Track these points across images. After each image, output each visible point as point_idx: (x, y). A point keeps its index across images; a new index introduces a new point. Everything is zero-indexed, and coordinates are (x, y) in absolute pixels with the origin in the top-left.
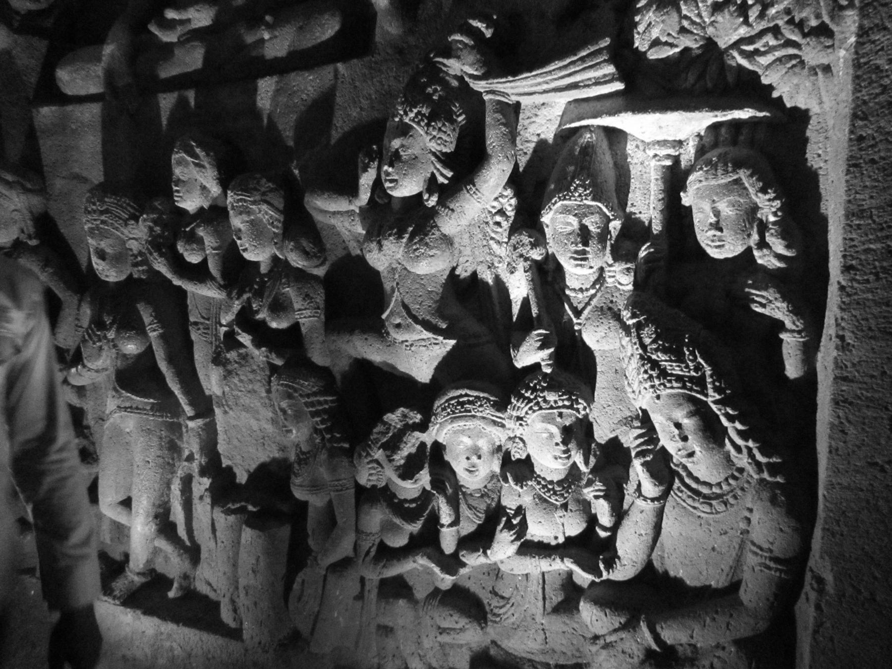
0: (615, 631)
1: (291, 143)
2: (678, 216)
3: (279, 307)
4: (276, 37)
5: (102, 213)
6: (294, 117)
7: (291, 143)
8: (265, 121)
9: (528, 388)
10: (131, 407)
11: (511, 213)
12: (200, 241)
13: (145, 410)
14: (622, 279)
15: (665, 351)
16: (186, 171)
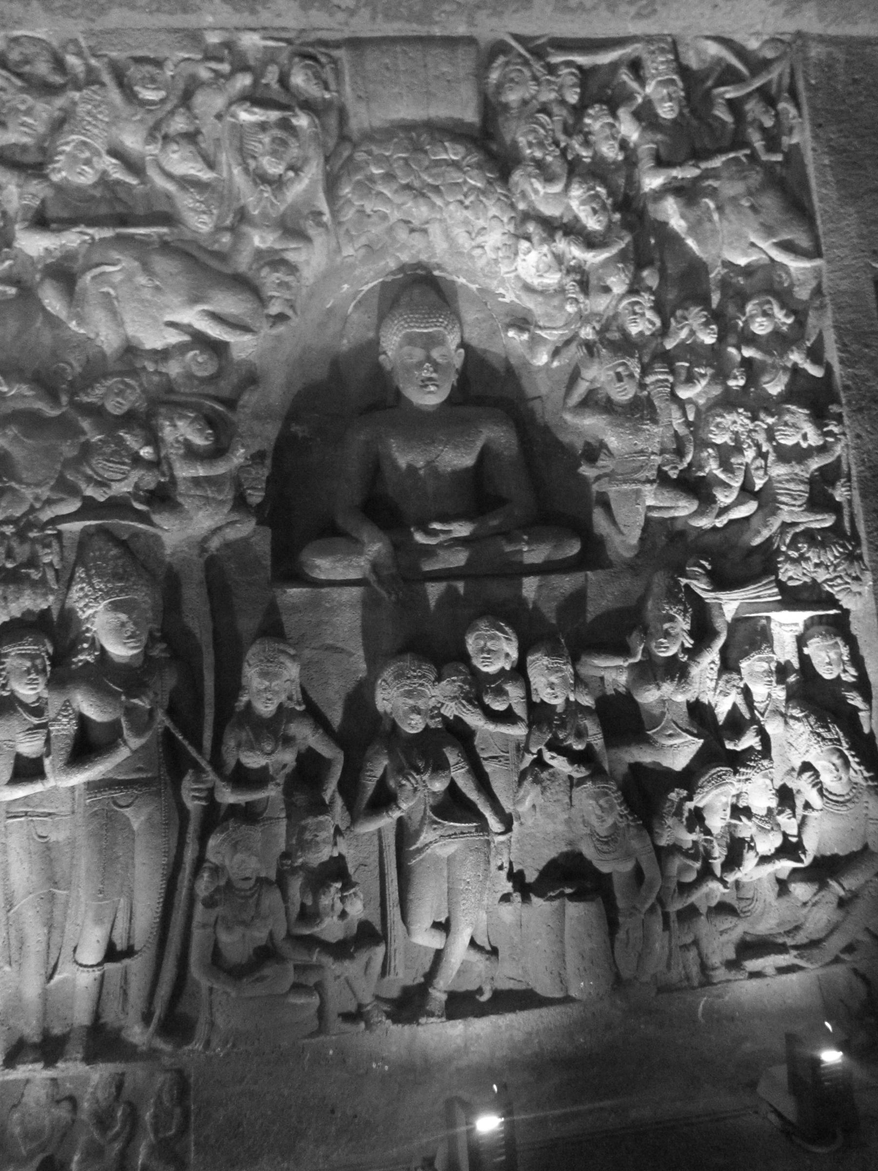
0: (815, 894)
1: (554, 621)
2: (805, 660)
3: (580, 734)
5: (420, 677)
6: (554, 604)
7: (554, 621)
8: (531, 606)
9: (751, 760)
11: (718, 662)
14: (780, 693)
15: (822, 727)
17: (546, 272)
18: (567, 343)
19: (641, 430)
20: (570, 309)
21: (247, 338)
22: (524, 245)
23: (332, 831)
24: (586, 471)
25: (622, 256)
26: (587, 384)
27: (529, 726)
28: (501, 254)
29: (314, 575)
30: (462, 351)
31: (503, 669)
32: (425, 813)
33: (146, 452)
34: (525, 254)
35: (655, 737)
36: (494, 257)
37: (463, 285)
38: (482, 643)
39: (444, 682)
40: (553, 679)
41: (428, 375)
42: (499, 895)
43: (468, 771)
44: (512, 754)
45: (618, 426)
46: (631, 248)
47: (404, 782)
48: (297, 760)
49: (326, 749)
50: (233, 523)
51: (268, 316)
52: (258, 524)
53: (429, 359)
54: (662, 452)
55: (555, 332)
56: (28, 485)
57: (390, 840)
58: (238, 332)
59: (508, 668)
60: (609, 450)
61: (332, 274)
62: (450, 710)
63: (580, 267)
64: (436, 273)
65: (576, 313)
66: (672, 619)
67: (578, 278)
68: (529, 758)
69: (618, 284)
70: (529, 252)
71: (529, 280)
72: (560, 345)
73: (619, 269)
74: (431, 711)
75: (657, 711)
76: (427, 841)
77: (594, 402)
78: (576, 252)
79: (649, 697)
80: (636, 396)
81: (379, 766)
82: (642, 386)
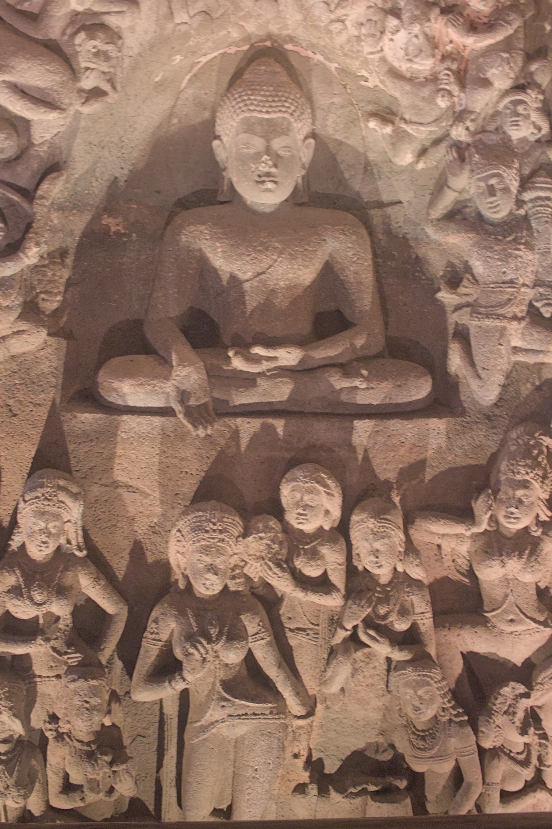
4: (372, 388)
5: (221, 532)
10: (246, 714)
12: (322, 558)
13: (264, 714)
16: (316, 498)
17: (416, 56)
18: (437, 142)
19: (510, 255)
20: (442, 103)
21: (53, 116)
22: (392, 22)
23: (107, 697)
24: (445, 296)
25: (507, 45)
26: (456, 194)
27: (346, 597)
28: (364, 31)
29: (111, 399)
30: (311, 141)
31: (321, 528)
32: (213, 688)
34: (393, 34)
35: (493, 620)
36: (356, 33)
37: (319, 64)
38: (298, 496)
39: (250, 539)
40: (378, 545)
41: (266, 169)
42: (293, 785)
43: (269, 644)
44: (323, 628)
45: (485, 248)
46: (521, 35)
47: (192, 650)
48: (73, 614)
49: (108, 604)
50: (18, 333)
51: (81, 91)
52: (49, 335)
53: (268, 150)
54: (537, 283)
55: (422, 128)
57: (172, 710)
58: (43, 110)
59: (327, 527)
60: (473, 275)
61: (159, 45)
62: (256, 571)
63: (459, 53)
64: (289, 47)
65: (448, 108)
66: (525, 485)
67: (454, 66)
68: (341, 635)
69: (501, 77)
70: (398, 31)
71: (396, 64)
72: (427, 144)
73: (503, 59)
74: (233, 570)
75: (498, 592)
76: (214, 720)
77: (460, 216)
78: (453, 36)
79: (491, 574)
80: (510, 213)
81: (165, 627)
82: (520, 203)
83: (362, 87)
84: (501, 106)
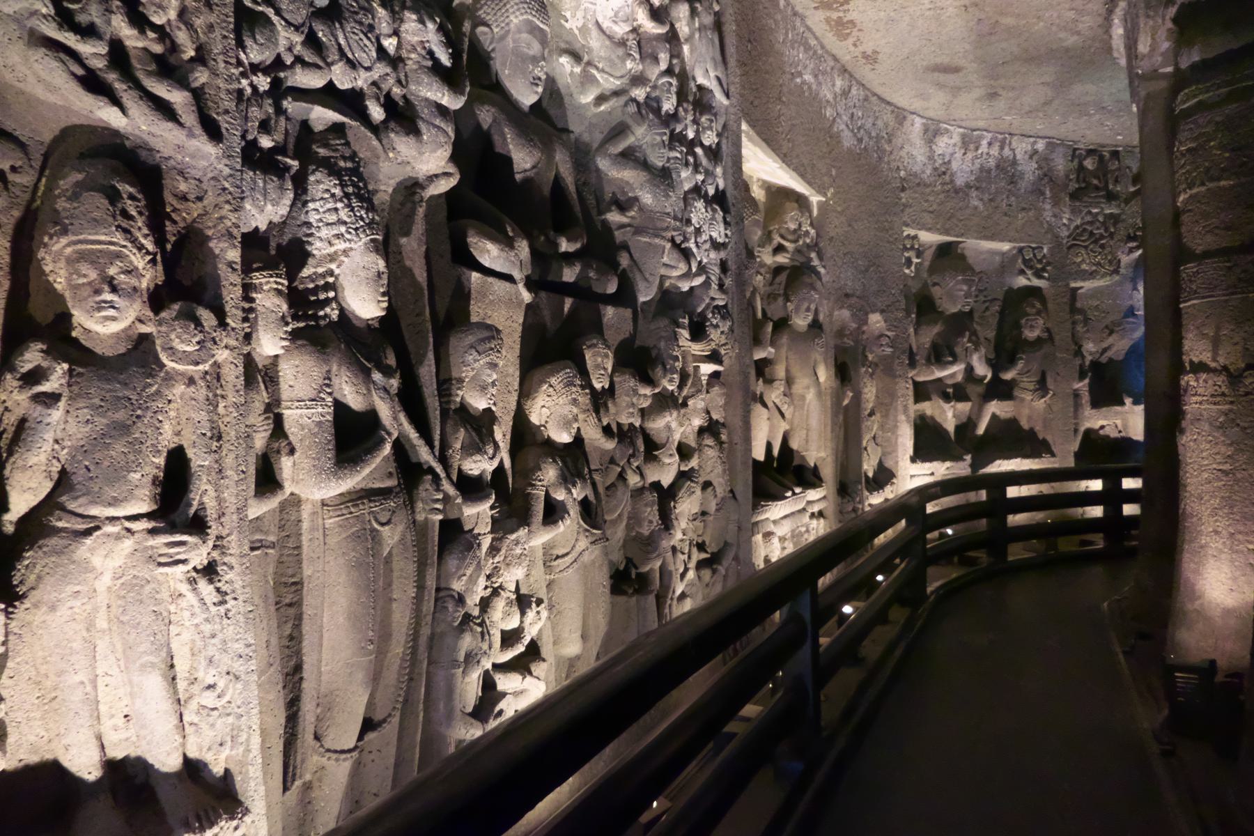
18: (616, 93)
29: (481, 260)
33: (390, 44)
56: (289, 24)
71: (600, 21)
77: (630, 157)
83: (562, 26)
84: (660, 82)
